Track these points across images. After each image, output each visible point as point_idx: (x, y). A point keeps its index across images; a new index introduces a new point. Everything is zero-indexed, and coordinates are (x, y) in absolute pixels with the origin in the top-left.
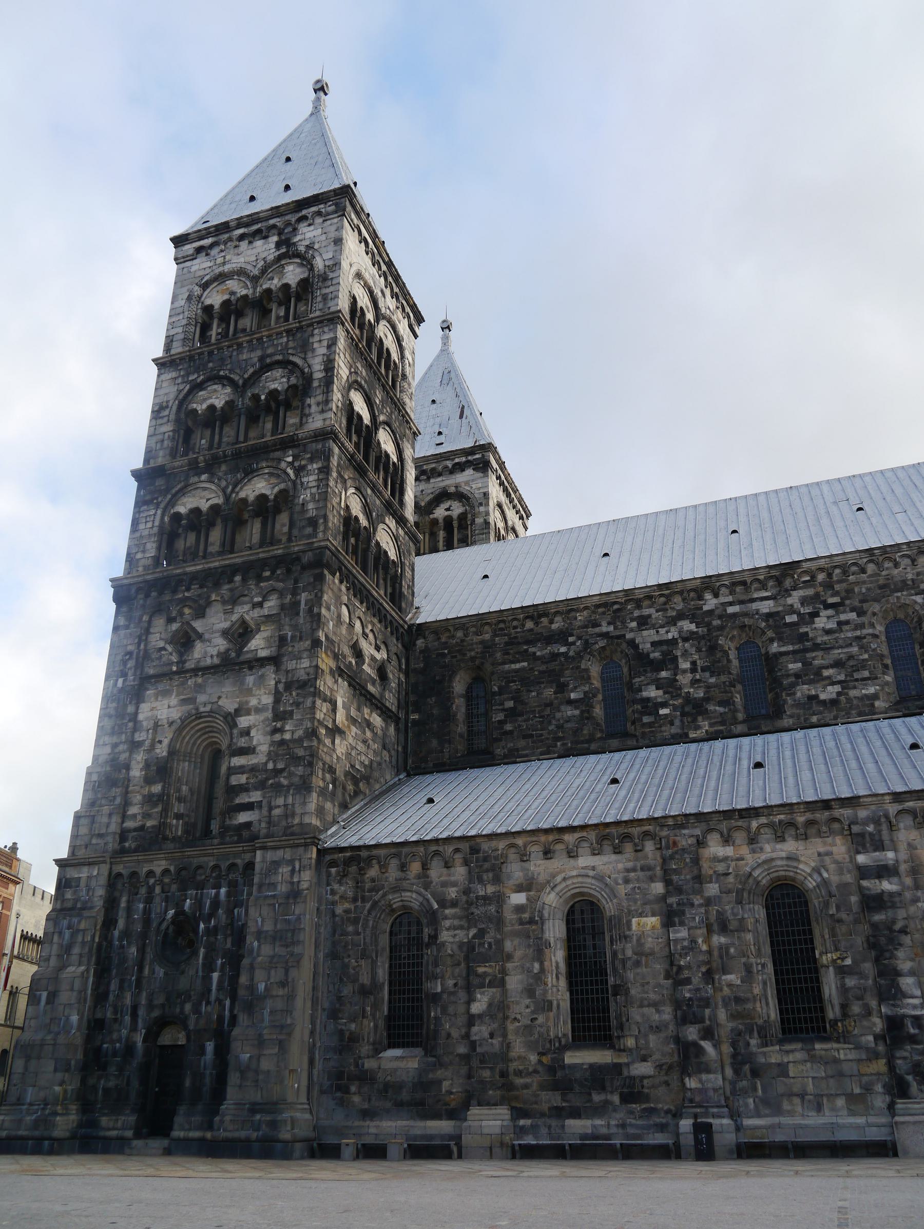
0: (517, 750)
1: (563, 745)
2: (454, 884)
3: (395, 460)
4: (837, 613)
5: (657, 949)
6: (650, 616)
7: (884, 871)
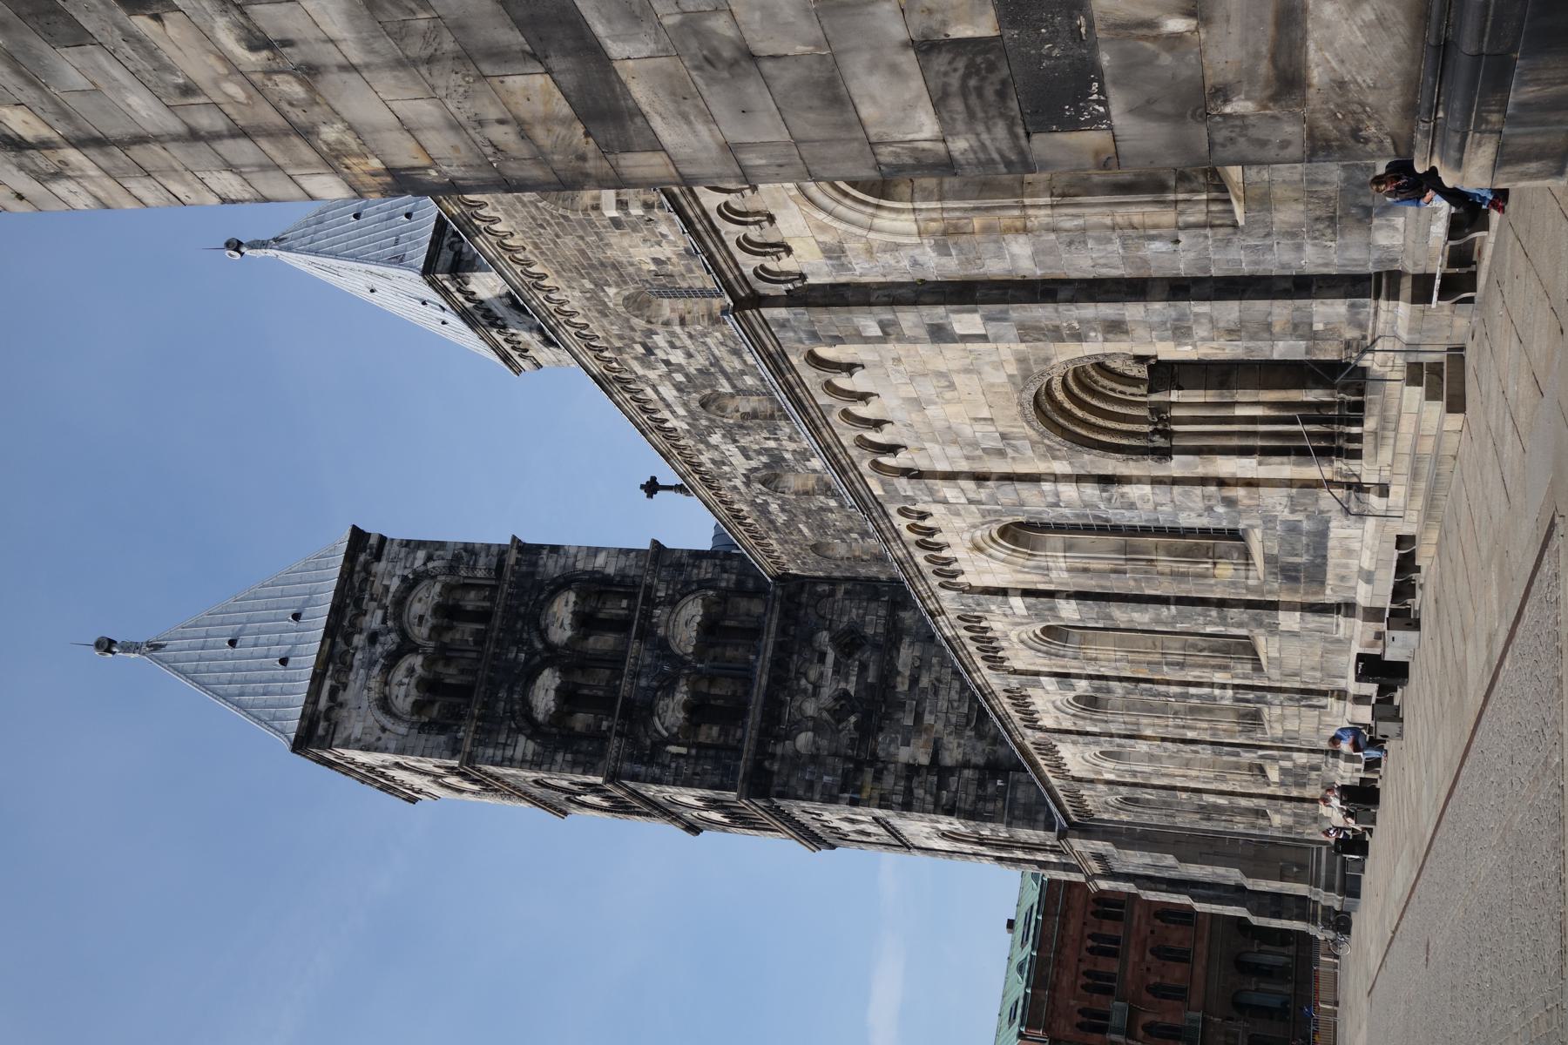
3: (572, 597)
4: (658, 347)
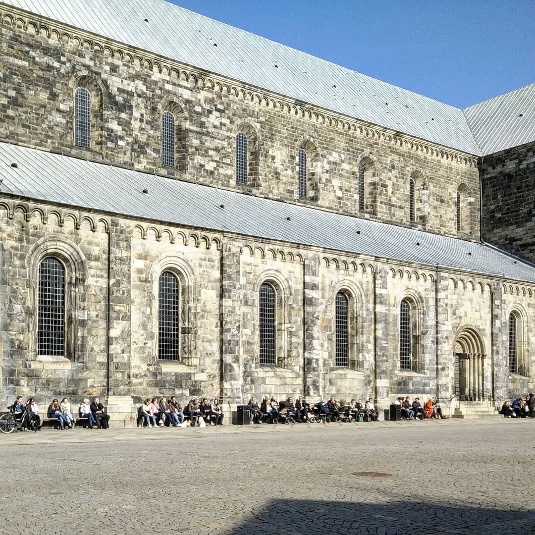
0: (17, 135)
1: (52, 143)
2: (97, 245)
5: (213, 310)
6: (118, 67)
7: (314, 287)
